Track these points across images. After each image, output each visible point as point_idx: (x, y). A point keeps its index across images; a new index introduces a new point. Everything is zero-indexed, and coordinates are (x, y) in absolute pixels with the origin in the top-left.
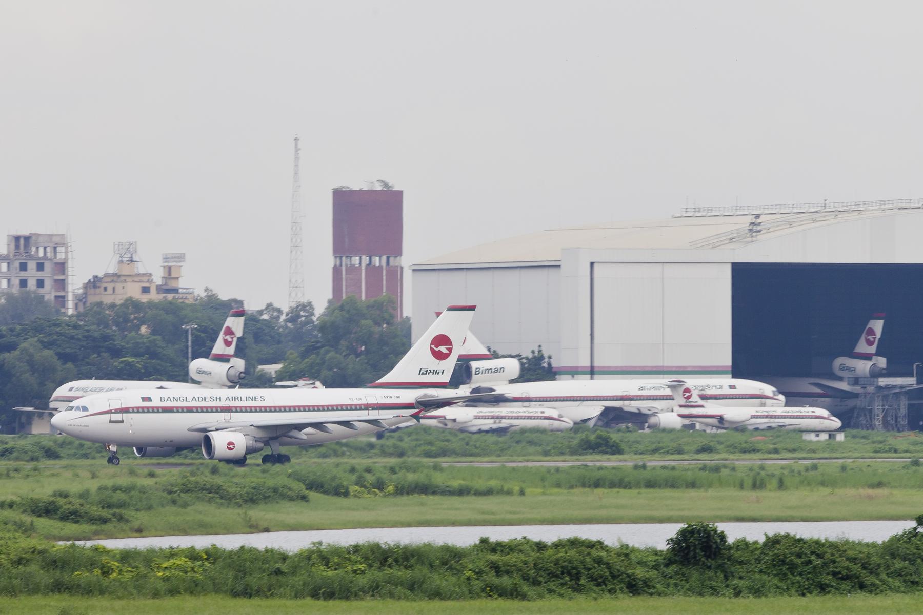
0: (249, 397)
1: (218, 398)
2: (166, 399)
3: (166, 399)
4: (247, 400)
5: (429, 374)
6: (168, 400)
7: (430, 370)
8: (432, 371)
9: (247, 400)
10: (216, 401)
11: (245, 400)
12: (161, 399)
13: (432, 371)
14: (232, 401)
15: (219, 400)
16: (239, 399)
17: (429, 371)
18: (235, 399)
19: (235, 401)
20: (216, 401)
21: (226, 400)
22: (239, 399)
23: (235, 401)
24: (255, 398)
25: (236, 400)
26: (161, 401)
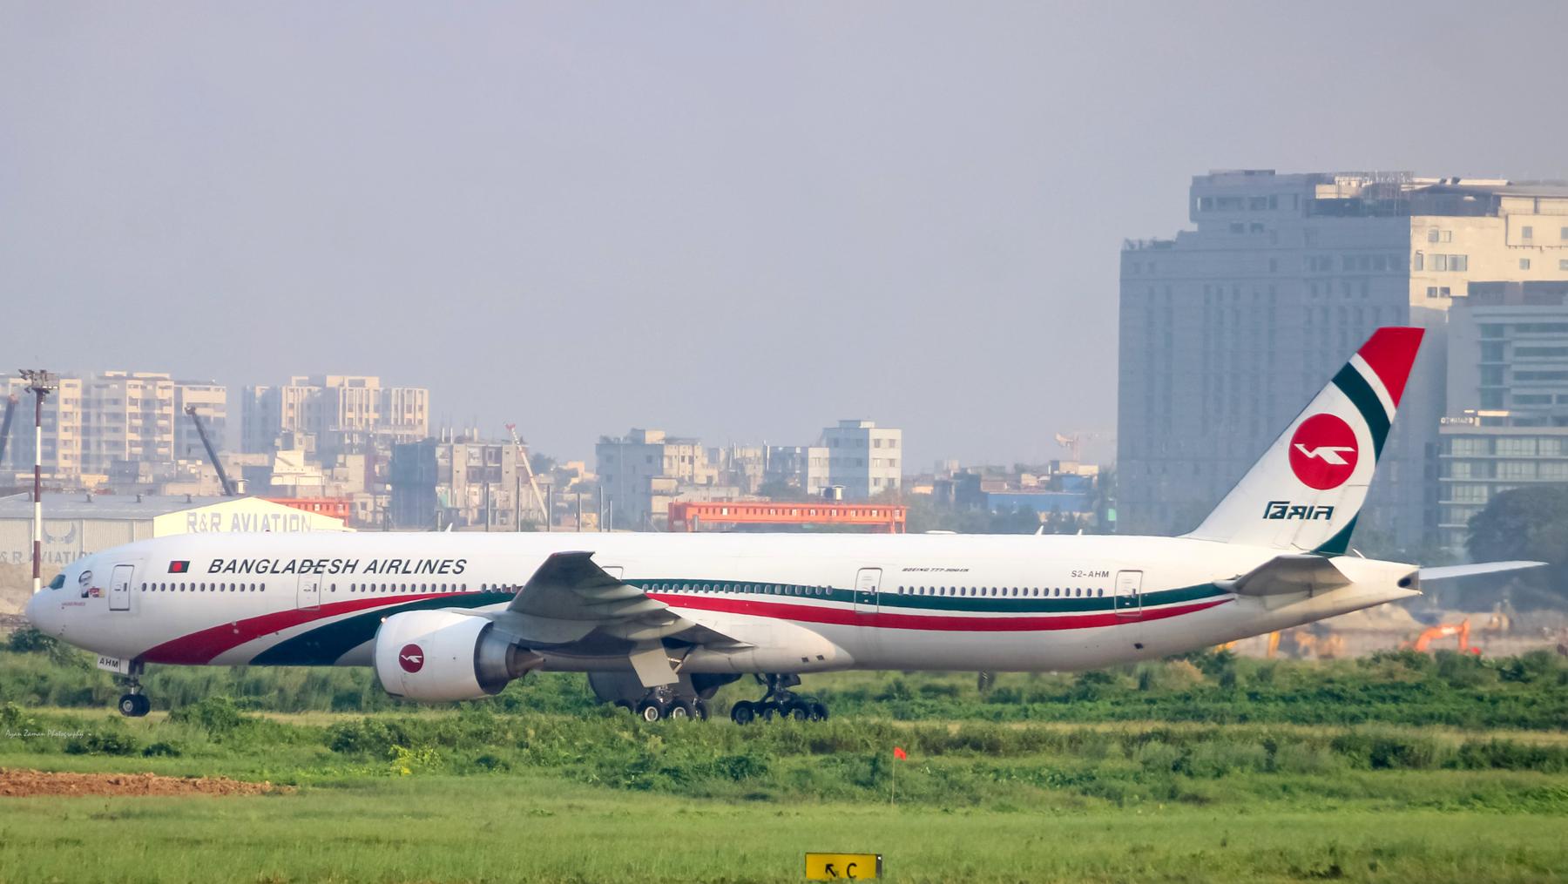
0: (429, 562)
1: (352, 563)
2: (224, 567)
3: (224, 567)
4: (416, 572)
5: (1290, 517)
6: (228, 568)
7: (1293, 508)
8: (1300, 510)
9: (416, 572)
10: (343, 572)
11: (413, 570)
12: (213, 565)
13: (1300, 510)
14: (380, 572)
15: (349, 569)
16: (401, 568)
17: (1290, 511)
18: (391, 566)
19: (388, 572)
20: (343, 572)
21: (369, 569)
22: (401, 568)
23: (388, 572)
24: (443, 566)
25: (393, 570)
26: (210, 571)
